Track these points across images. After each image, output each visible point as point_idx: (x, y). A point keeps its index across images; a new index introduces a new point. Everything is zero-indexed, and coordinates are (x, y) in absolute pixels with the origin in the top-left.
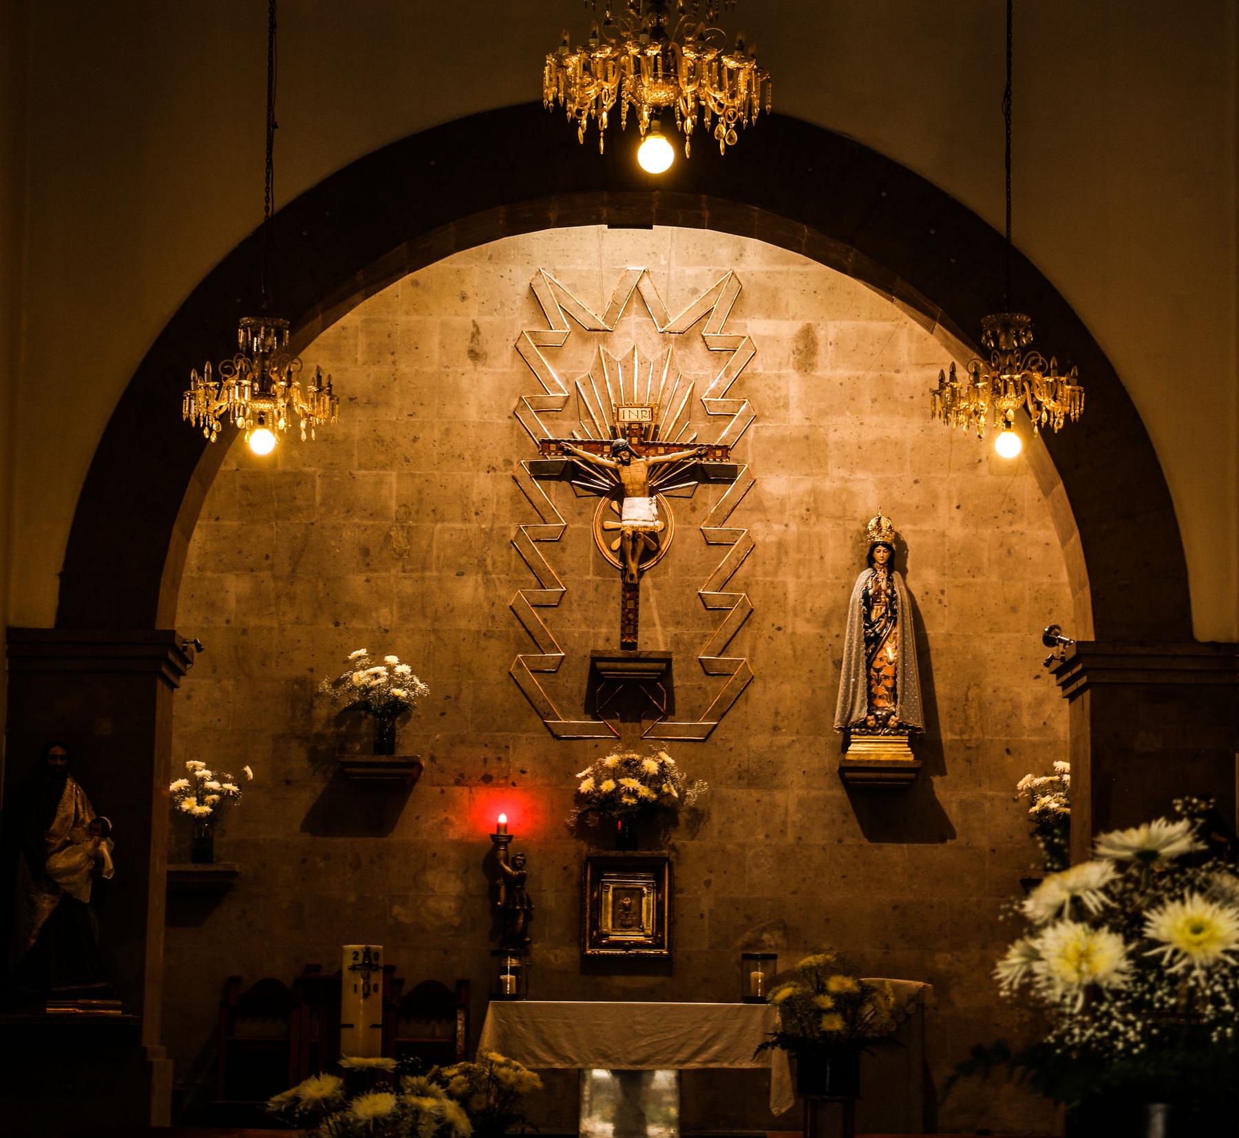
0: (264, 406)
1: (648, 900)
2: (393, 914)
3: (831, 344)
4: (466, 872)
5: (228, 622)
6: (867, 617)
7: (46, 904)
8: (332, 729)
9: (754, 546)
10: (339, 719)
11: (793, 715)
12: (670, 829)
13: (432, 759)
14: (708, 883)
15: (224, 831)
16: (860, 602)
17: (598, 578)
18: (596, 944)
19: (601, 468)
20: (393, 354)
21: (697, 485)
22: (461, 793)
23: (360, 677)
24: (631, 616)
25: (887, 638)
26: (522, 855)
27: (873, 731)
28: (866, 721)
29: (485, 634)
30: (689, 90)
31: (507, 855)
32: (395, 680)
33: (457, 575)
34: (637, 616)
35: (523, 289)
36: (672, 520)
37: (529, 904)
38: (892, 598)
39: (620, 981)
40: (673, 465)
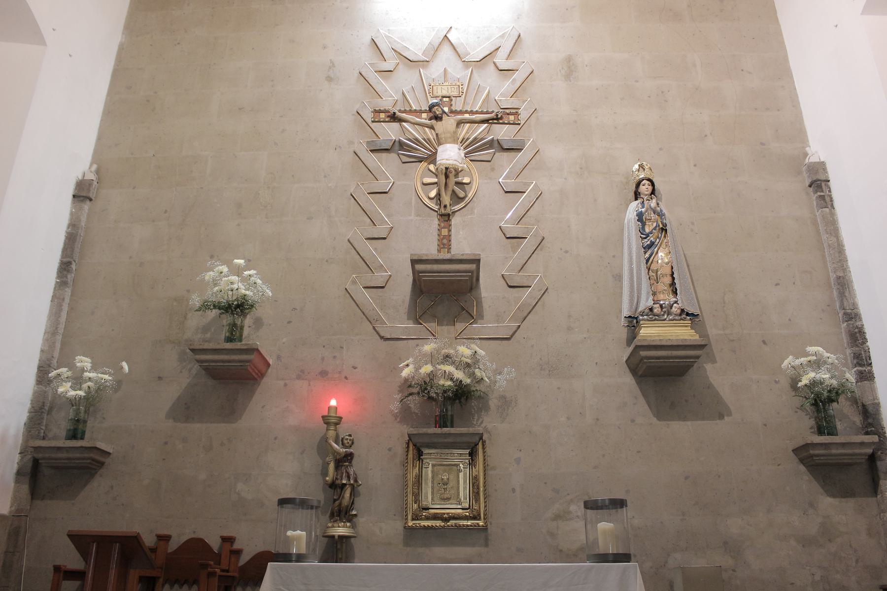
1: (465, 475)
2: (237, 491)
3: (586, 66)
4: (302, 453)
5: (130, 258)
6: (642, 231)
8: (199, 336)
9: (541, 194)
10: (205, 329)
11: (583, 317)
12: (483, 413)
13: (279, 358)
14: (518, 461)
15: (104, 418)
16: (634, 219)
17: (418, 218)
18: (416, 517)
20: (272, 81)
21: (495, 154)
24: (445, 241)
25: (661, 245)
26: (350, 436)
28: (651, 309)
29: (327, 261)
31: (337, 436)
33: (308, 219)
34: (450, 241)
35: (367, 40)
36: (476, 176)
37: (356, 481)
38: (661, 215)
39: (439, 551)
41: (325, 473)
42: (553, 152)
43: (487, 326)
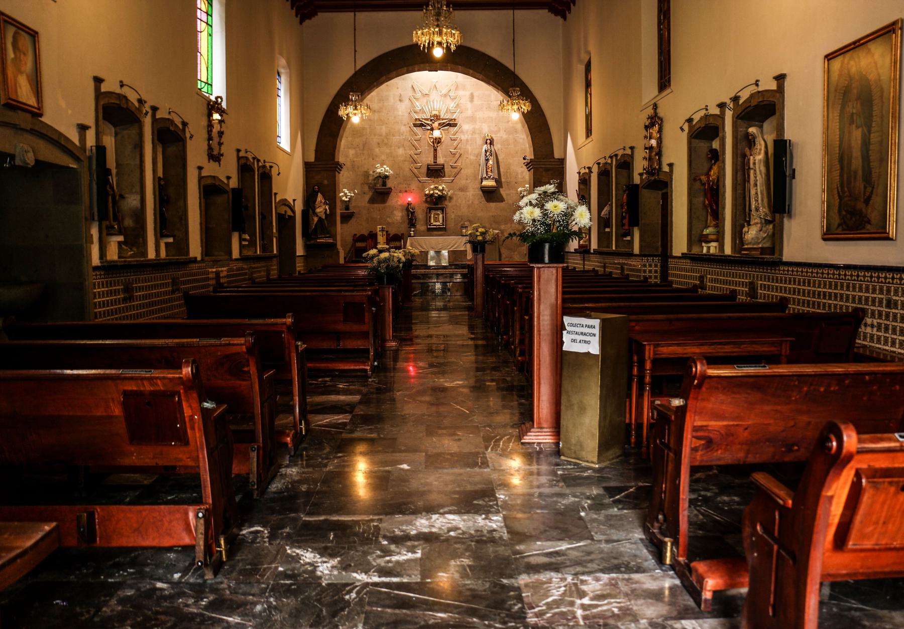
0: (356, 112)
7: (316, 219)
10: (374, 180)
19: (428, 124)
22: (400, 194)
23: (378, 170)
27: (487, 179)
30: (445, 38)
32: (386, 171)
35: (410, 86)
40: (444, 123)
41: (408, 216)
42: (466, 127)
43: (446, 179)
